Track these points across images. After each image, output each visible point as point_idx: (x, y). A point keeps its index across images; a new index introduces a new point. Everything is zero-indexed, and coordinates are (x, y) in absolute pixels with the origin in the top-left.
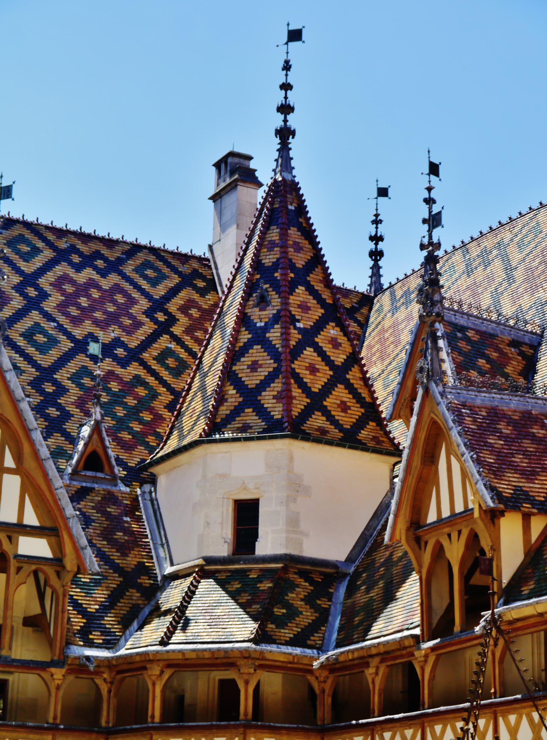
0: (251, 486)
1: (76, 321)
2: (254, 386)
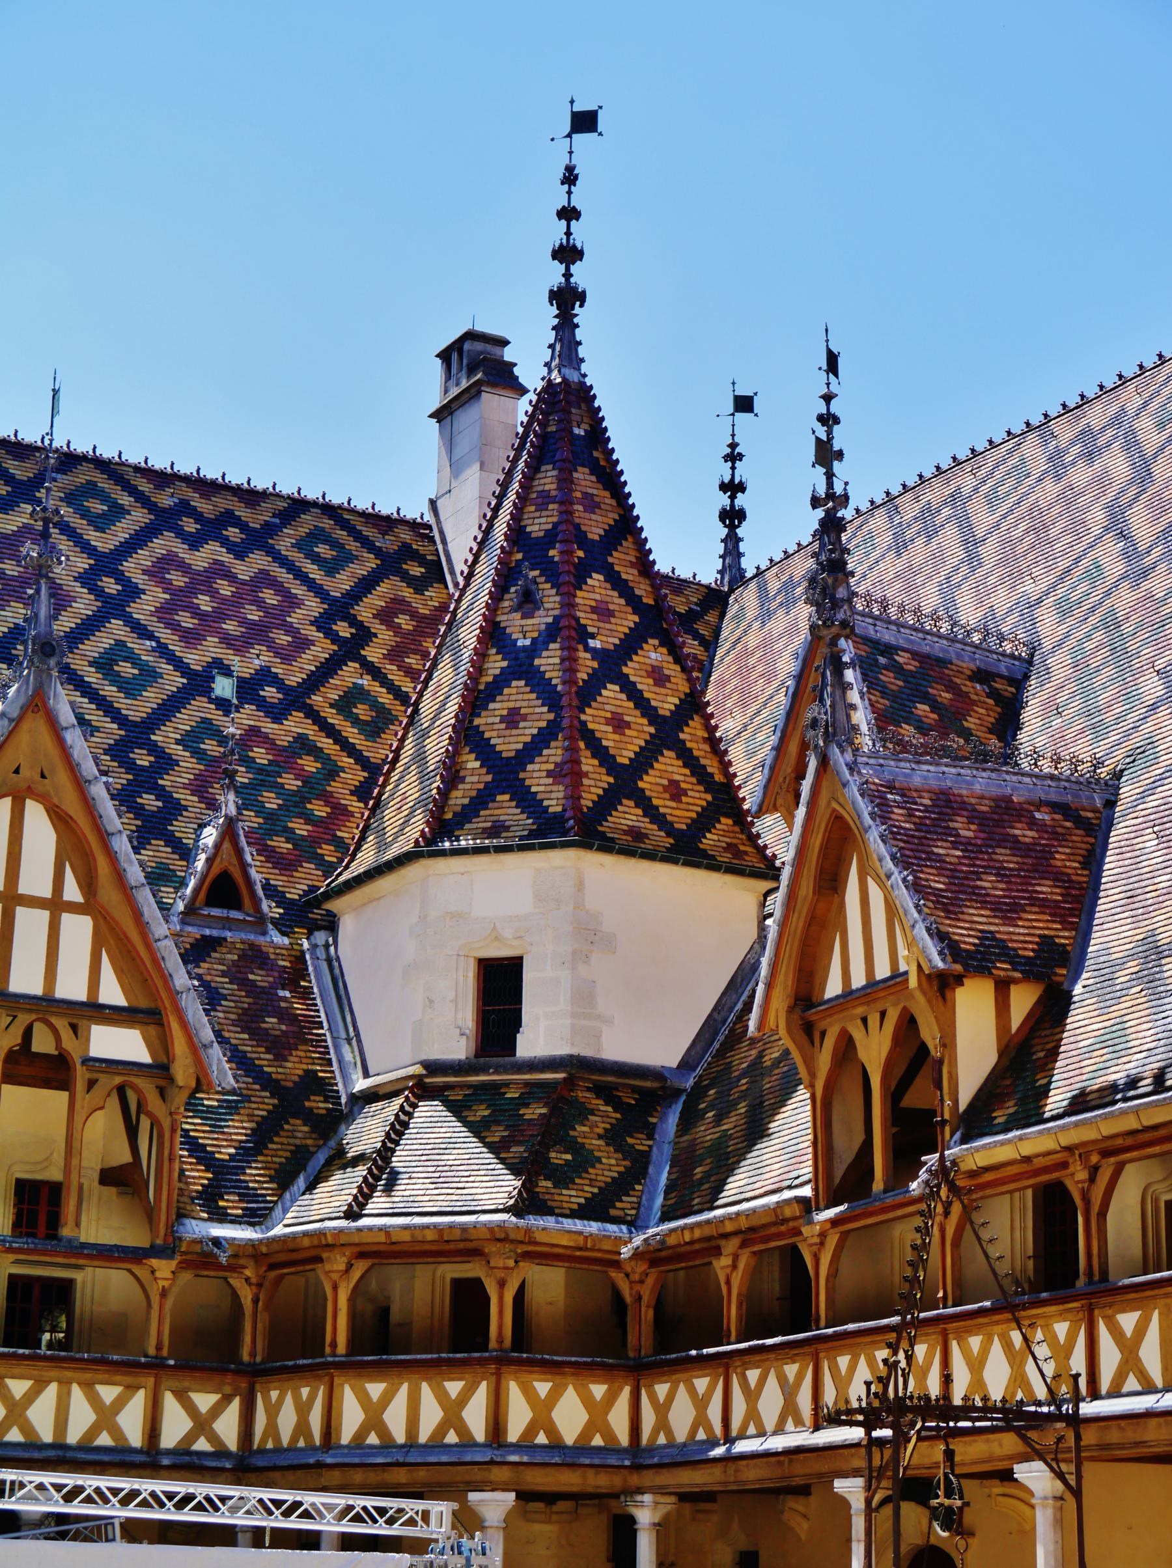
0: (508, 934)
1: (191, 638)
2: (512, 754)
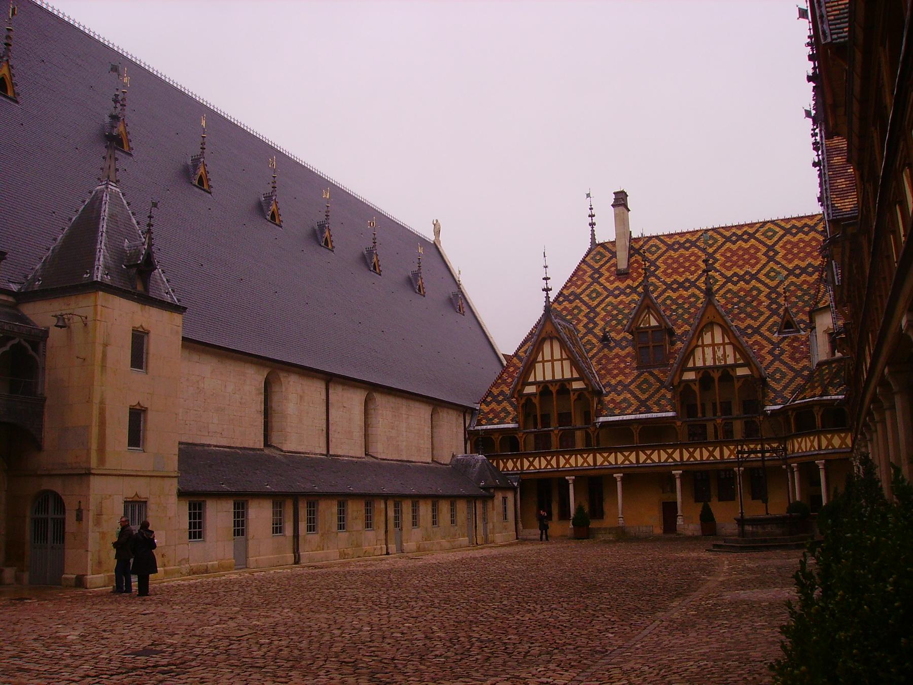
1: (790, 261)
